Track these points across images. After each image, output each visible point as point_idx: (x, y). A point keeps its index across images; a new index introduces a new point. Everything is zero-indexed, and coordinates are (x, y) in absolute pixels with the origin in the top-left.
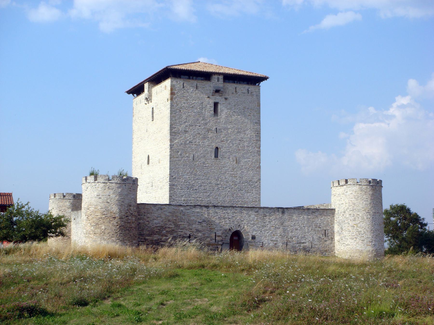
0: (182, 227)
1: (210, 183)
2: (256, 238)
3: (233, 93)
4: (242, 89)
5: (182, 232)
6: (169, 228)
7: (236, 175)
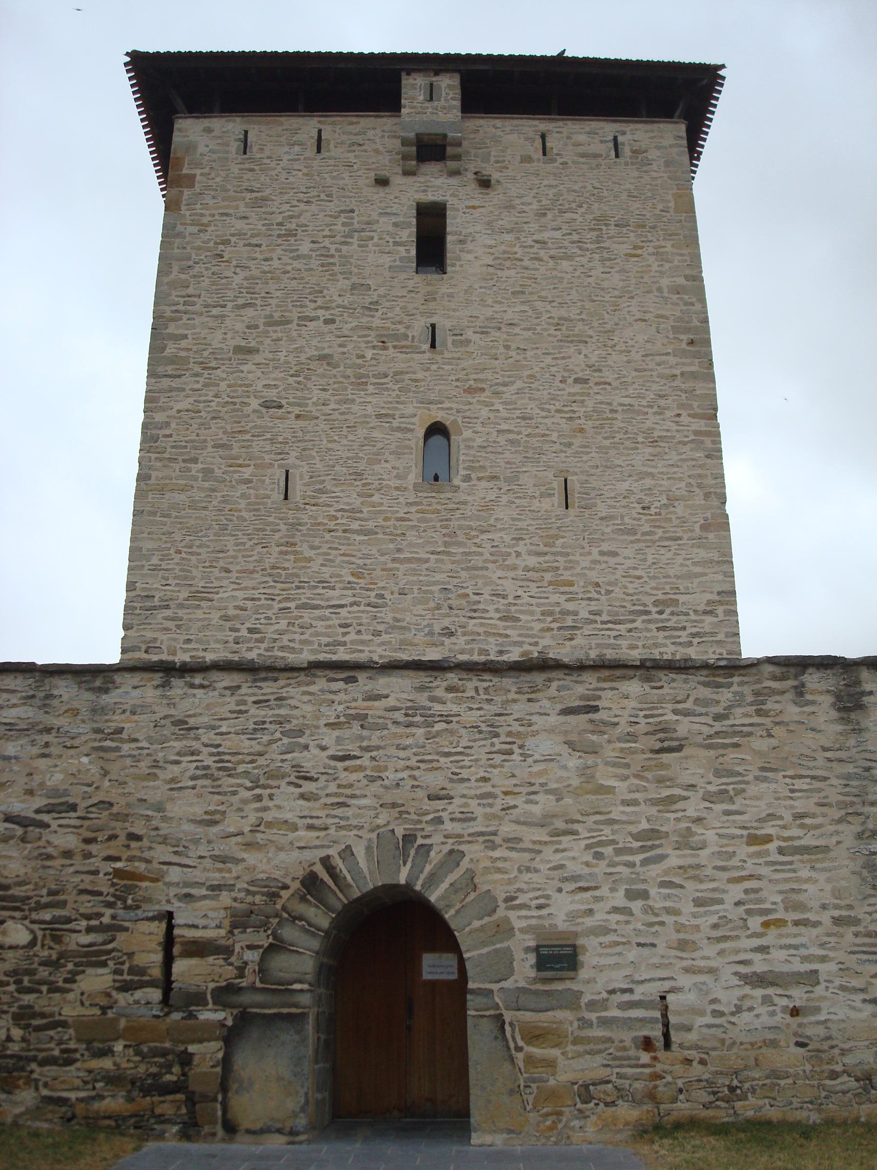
2: (589, 959)
3: (527, 159)
4: (582, 138)
7: (567, 575)
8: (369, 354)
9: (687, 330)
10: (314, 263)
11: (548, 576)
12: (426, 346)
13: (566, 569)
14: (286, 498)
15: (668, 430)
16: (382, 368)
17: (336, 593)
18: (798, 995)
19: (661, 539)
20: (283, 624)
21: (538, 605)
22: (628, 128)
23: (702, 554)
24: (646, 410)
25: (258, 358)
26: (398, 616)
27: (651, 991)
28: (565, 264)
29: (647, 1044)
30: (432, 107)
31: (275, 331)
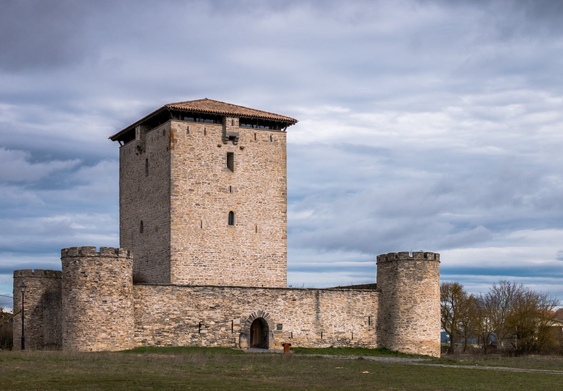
0: (190, 313)
1: (223, 257)
3: (251, 141)
4: (264, 136)
5: (190, 319)
6: (173, 314)
7: (256, 248)
8: (217, 193)
9: (282, 191)
10: (205, 168)
16: (220, 197)
18: (308, 333)
20: (202, 256)
22: (274, 133)
23: (281, 244)
25: (194, 192)
27: (290, 331)
29: (290, 338)
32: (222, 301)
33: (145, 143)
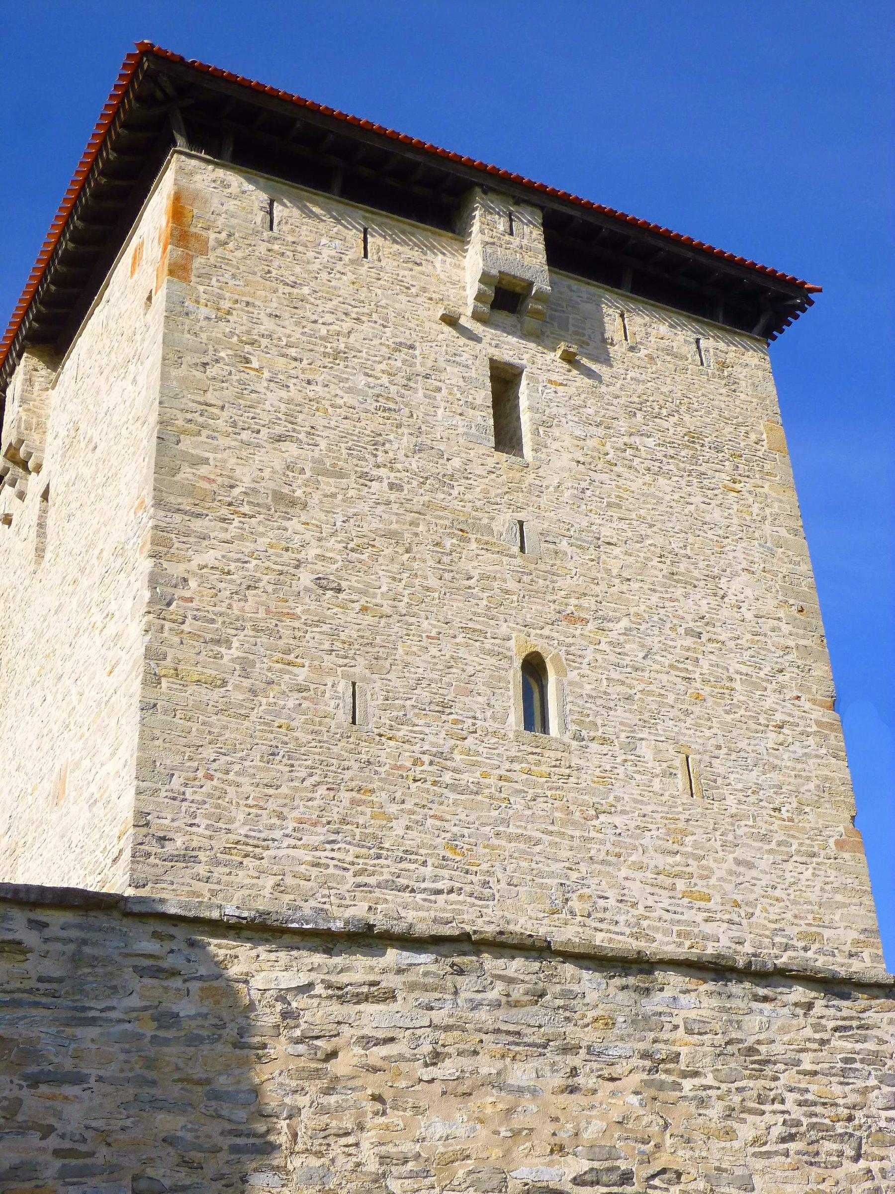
7: (701, 886)
11: (681, 885)
12: (516, 549)
13: (701, 877)
14: (354, 722)
15: (790, 715)
17: (428, 871)
19: (798, 852)
21: (672, 922)
24: (765, 684)
26: (509, 916)
28: (662, 481)
30: (502, 242)
31: (328, 484)
32: (650, 1122)
33: (41, 427)
